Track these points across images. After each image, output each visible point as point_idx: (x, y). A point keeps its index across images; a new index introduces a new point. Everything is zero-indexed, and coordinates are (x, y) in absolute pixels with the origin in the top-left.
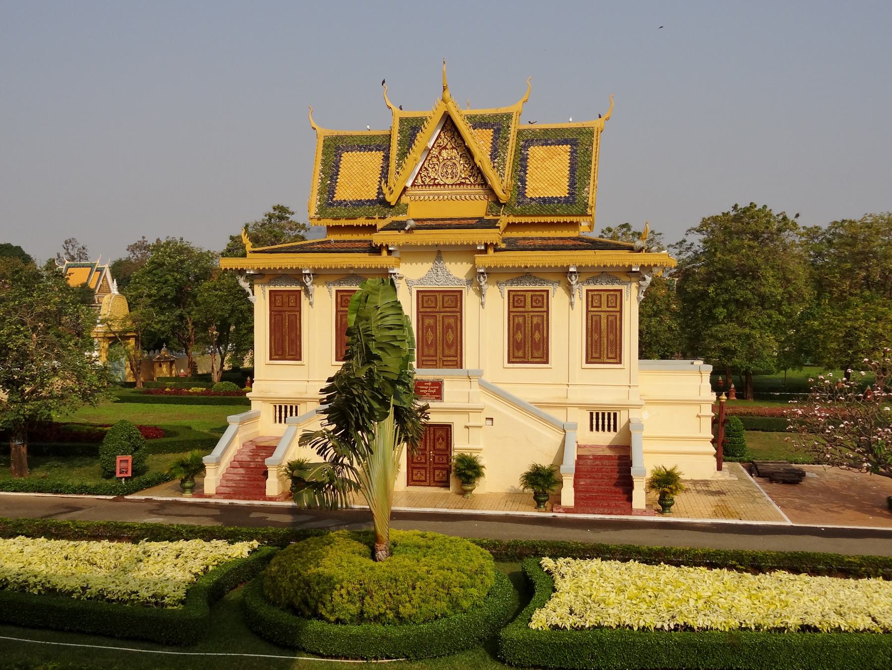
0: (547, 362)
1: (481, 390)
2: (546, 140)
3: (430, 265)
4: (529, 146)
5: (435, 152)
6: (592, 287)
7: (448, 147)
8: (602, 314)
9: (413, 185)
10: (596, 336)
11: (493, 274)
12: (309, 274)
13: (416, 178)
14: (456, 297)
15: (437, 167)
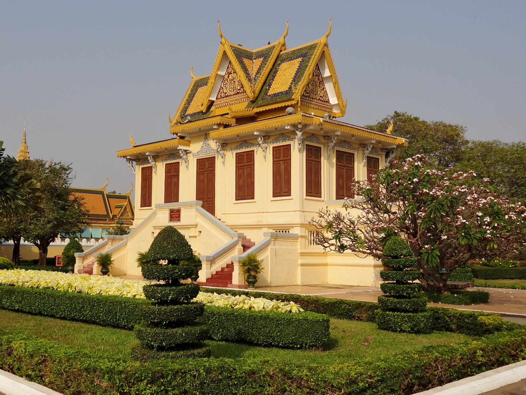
0: (253, 198)
1: (197, 214)
2: (291, 58)
3: (203, 142)
4: (282, 63)
5: (226, 77)
6: (276, 145)
7: (232, 72)
8: (281, 162)
9: (217, 99)
10: (278, 178)
11: (225, 144)
12: (149, 155)
13: (218, 95)
14: (211, 161)
15: (227, 86)
